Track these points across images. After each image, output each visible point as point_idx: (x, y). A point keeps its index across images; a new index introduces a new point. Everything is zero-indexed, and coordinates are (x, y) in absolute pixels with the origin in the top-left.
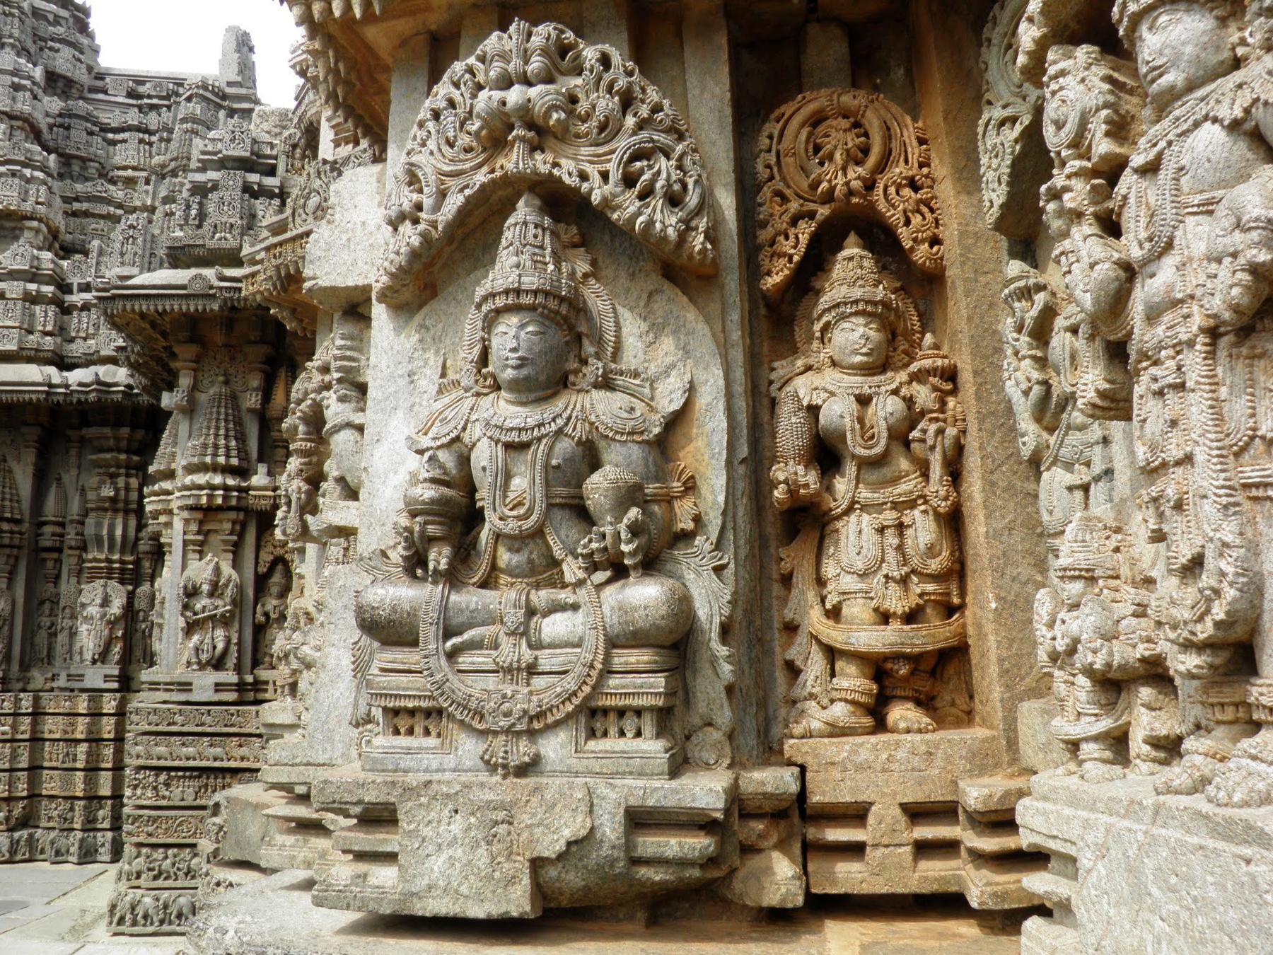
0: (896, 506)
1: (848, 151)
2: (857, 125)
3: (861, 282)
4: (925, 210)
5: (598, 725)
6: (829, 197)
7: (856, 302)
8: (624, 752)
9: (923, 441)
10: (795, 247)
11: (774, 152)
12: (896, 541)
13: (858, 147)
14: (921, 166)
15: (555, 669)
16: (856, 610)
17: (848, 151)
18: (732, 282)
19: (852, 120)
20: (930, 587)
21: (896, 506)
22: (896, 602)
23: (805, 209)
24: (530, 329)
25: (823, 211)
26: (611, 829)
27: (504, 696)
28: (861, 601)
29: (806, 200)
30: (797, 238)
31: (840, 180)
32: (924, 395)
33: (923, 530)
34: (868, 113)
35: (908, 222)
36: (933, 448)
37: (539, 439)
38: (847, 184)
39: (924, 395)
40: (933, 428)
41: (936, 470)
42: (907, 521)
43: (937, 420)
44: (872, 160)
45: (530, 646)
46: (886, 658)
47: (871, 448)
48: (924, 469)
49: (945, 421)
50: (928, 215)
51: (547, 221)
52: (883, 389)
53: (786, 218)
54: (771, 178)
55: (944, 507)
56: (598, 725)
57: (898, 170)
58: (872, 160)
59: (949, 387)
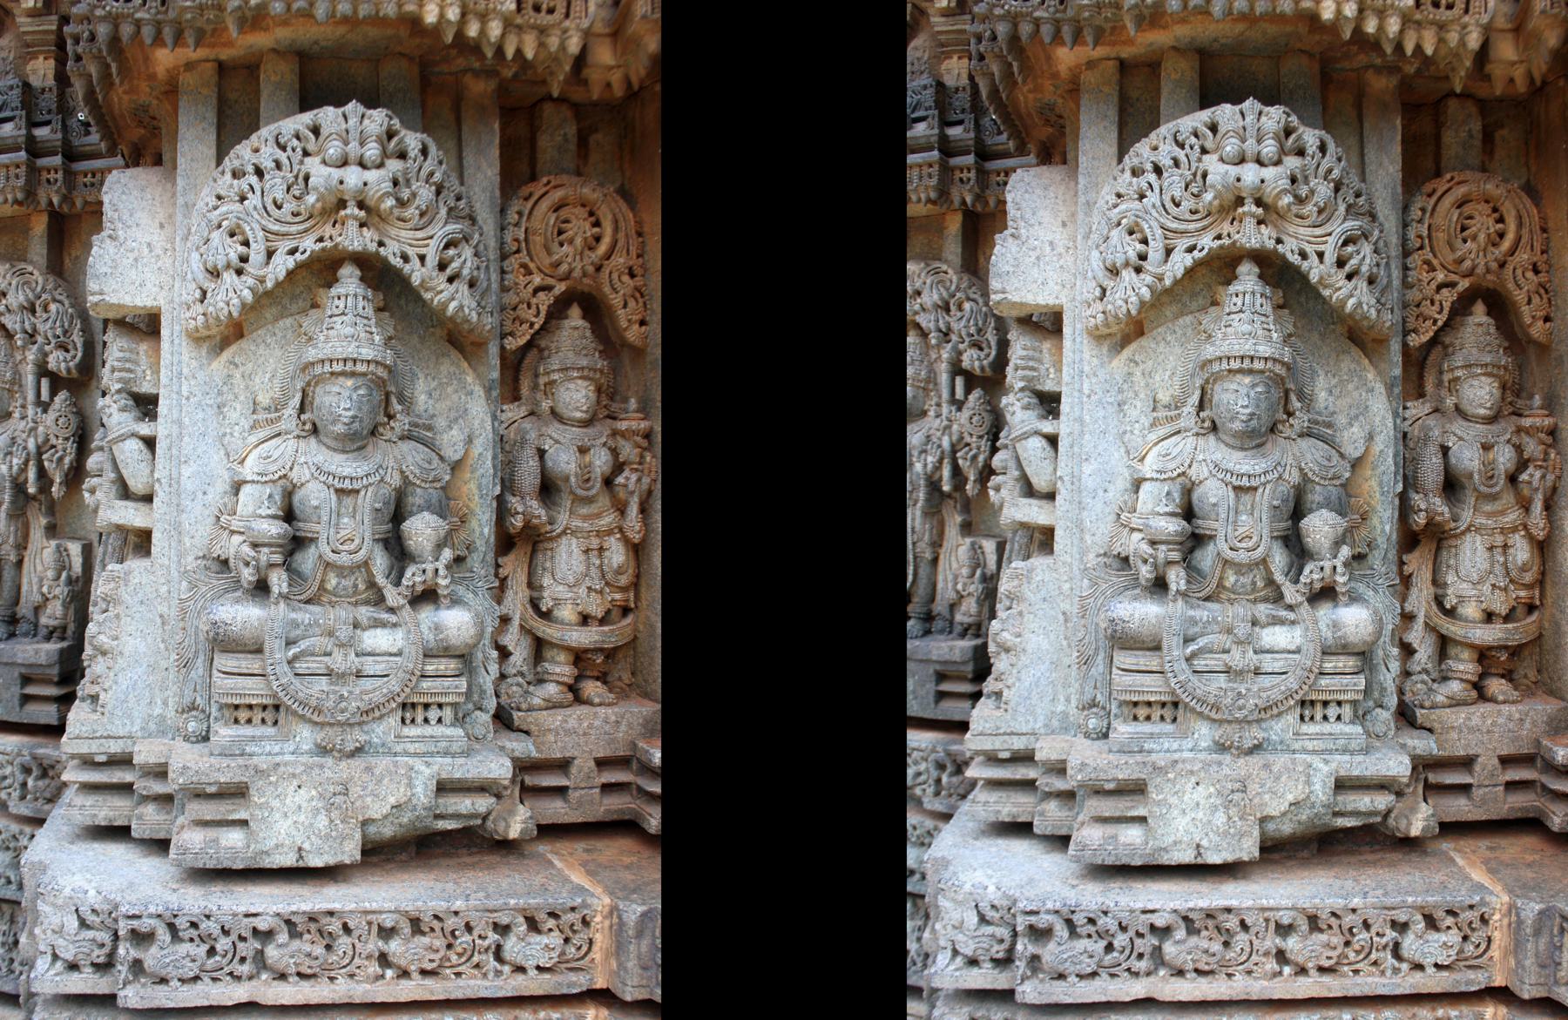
0: (1503, 531)
1: (1489, 235)
2: (1495, 210)
3: (1488, 349)
4: (1542, 291)
5: (1307, 713)
6: (1469, 274)
7: (1486, 365)
8: (1331, 734)
9: (1530, 483)
10: (1440, 313)
11: (1426, 226)
12: (1502, 559)
13: (1496, 231)
14: (1542, 253)
15: (1276, 670)
16: (1471, 610)
17: (1489, 235)
18: (1395, 346)
19: (1491, 205)
20: (1522, 594)
21: (1503, 531)
22: (1500, 605)
23: (1449, 279)
24: (1259, 389)
25: (1464, 284)
26: (1321, 791)
27: (1239, 693)
28: (1474, 604)
29: (1449, 271)
30: (1441, 304)
31: (1481, 261)
32: (1532, 447)
33: (1521, 552)
34: (1507, 203)
35: (1529, 302)
36: (1537, 489)
37: (1264, 484)
38: (1486, 264)
39: (1532, 447)
40: (1538, 474)
41: (1538, 507)
42: (1510, 542)
43: (1541, 467)
44: (1506, 244)
45: (1255, 652)
46: (1490, 648)
47: (1491, 486)
48: (1526, 507)
49: (1546, 468)
50: (1545, 296)
51: (1268, 290)
52: (1502, 439)
53: (1433, 285)
54: (1421, 248)
55: (1541, 535)
56: (1307, 713)
57: (1523, 256)
58: (1506, 244)
59: (1549, 440)
